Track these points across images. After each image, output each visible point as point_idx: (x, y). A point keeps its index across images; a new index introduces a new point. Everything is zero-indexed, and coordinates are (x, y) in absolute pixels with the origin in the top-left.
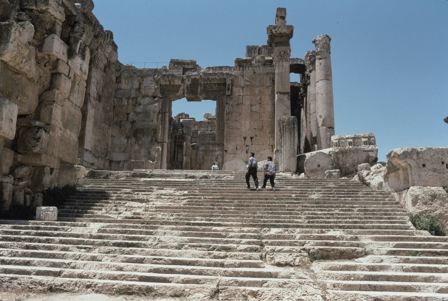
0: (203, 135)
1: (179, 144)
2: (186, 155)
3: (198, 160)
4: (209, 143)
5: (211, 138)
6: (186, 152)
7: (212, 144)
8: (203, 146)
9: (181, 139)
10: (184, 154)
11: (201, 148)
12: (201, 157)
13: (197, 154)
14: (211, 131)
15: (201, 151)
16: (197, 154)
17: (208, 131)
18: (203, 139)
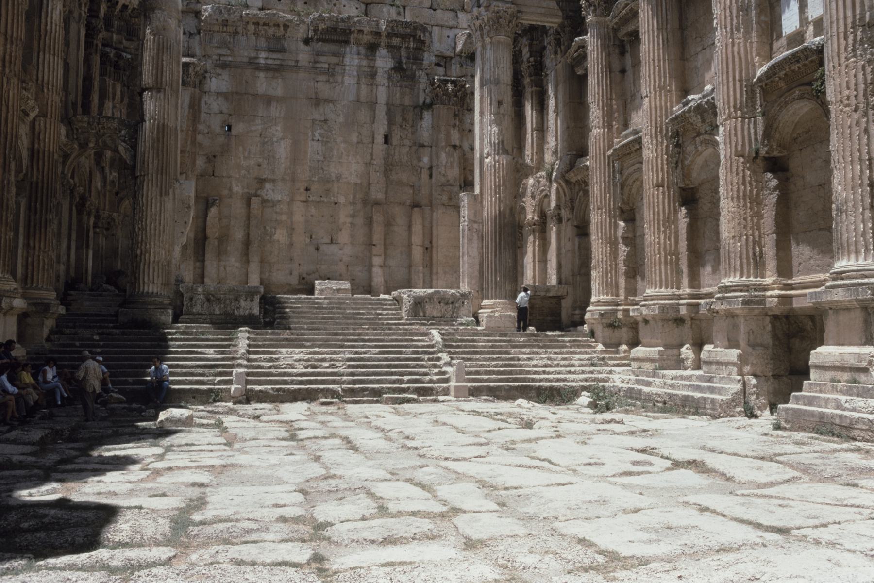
0: (225, 23)
1: (112, 53)
2: (158, 88)
3: (200, 138)
4: (253, 64)
5: (262, 43)
6: (159, 70)
7: (268, 69)
8: (225, 74)
9: (119, 32)
10: (147, 79)
11: (218, 83)
12: (216, 123)
13: (195, 107)
14: (262, 9)
15: (218, 94)
16: (195, 107)
17: (247, 7)
18: (224, 44)
